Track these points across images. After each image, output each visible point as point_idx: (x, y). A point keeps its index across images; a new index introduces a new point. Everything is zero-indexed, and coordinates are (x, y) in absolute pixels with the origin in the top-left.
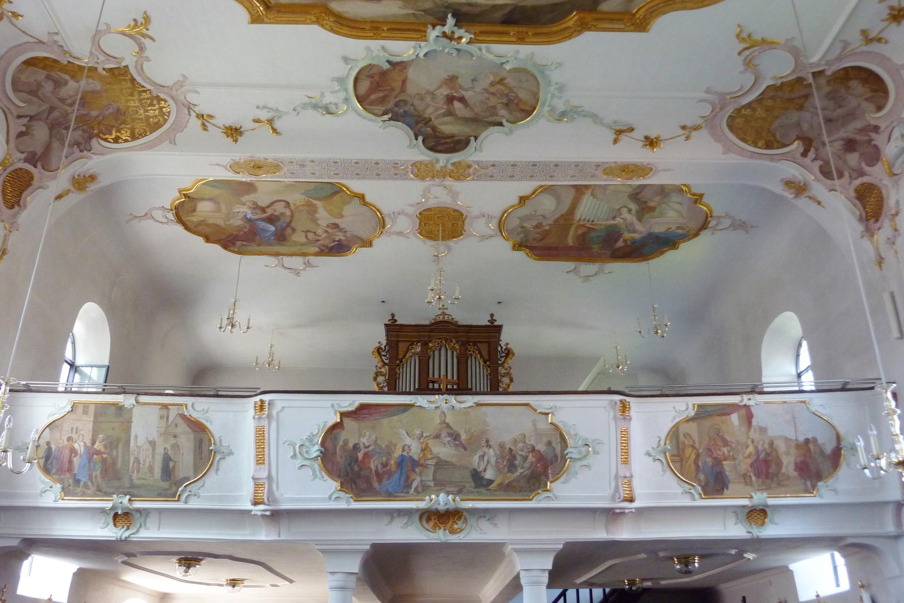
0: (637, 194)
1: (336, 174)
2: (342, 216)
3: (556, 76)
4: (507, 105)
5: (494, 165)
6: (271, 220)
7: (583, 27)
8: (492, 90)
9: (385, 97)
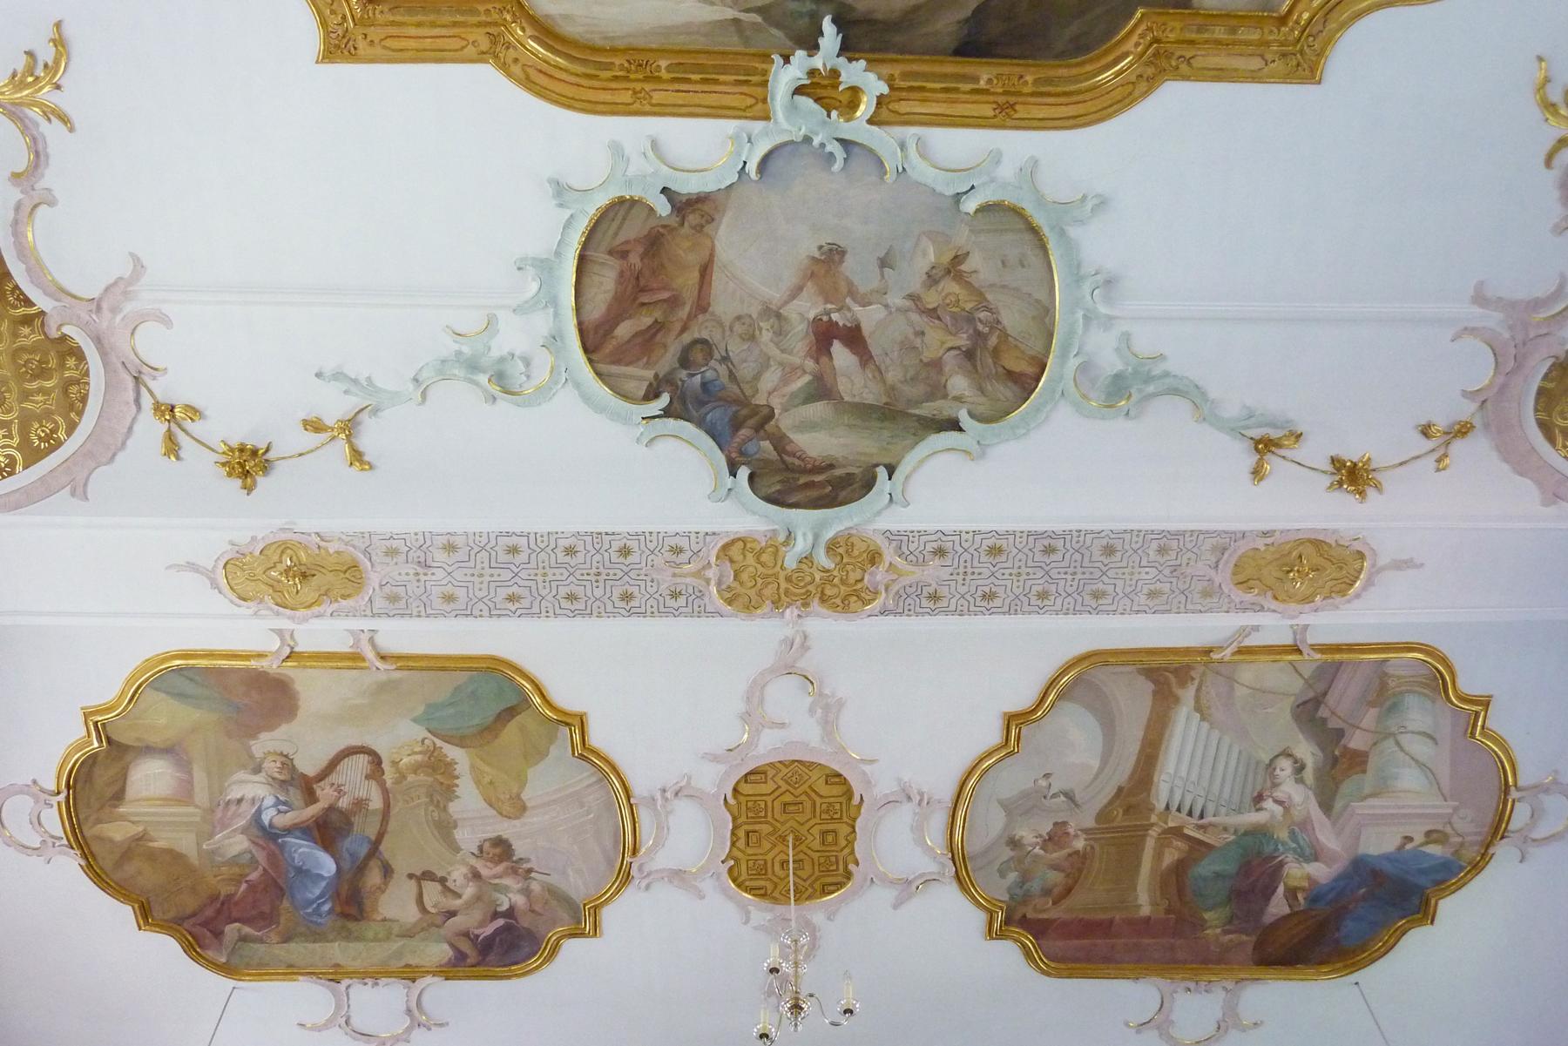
0: (1318, 701)
1: (512, 598)
2: (520, 809)
3: (1096, 244)
4: (969, 355)
5: (940, 552)
6: (327, 831)
7: (1162, 65)
8: (932, 299)
9: (658, 327)
